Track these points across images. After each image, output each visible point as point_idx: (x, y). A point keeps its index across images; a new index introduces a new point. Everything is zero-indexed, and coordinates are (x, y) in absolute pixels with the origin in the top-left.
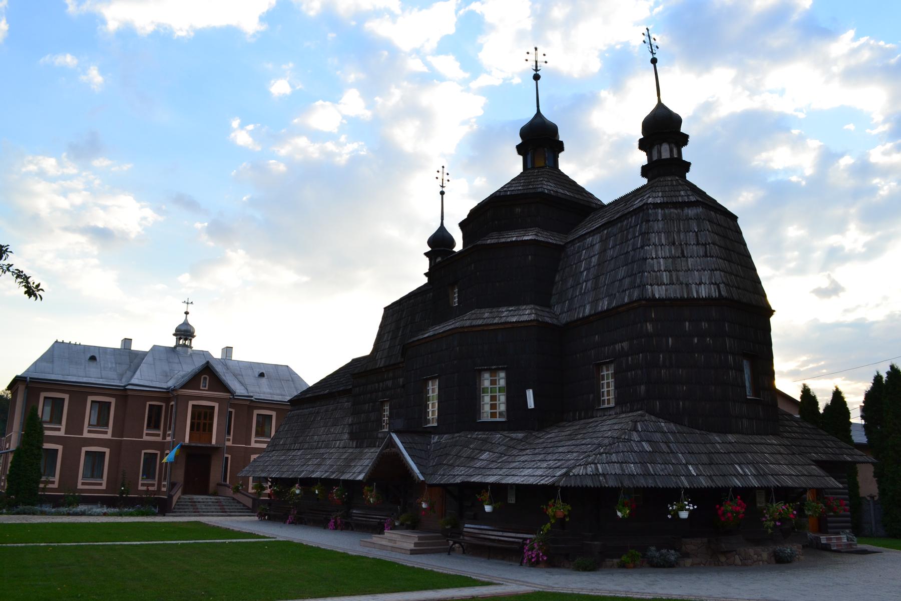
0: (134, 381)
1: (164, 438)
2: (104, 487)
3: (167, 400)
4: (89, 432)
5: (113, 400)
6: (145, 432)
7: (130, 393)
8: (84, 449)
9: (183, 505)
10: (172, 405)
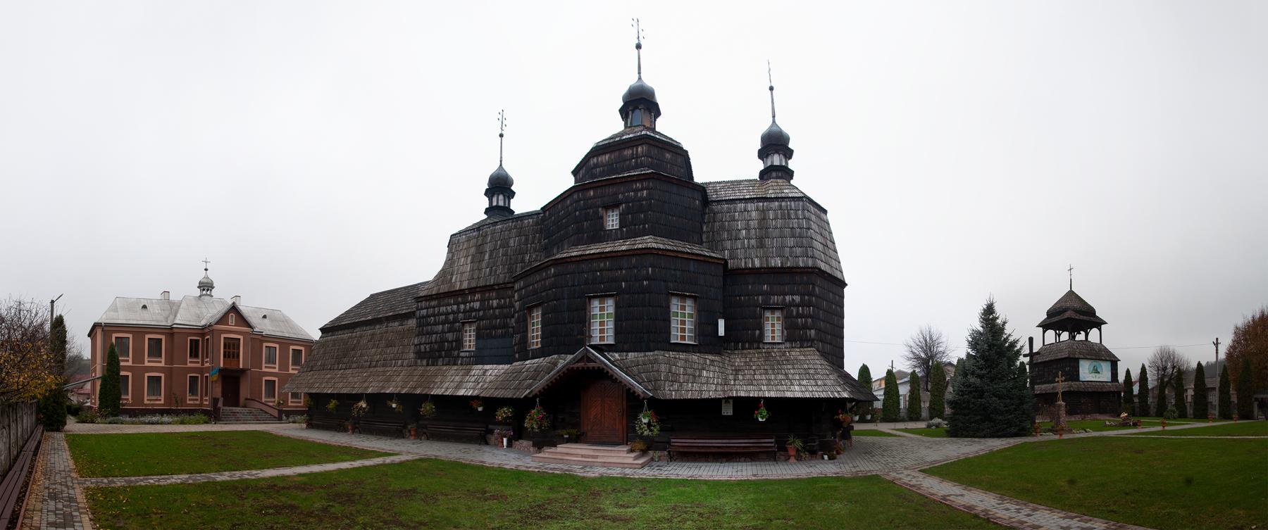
0: (177, 321)
1: (203, 364)
2: (162, 402)
3: (203, 335)
4: (149, 361)
5: (163, 337)
6: (189, 360)
7: (175, 330)
8: (147, 375)
9: (227, 415)
10: (208, 339)
